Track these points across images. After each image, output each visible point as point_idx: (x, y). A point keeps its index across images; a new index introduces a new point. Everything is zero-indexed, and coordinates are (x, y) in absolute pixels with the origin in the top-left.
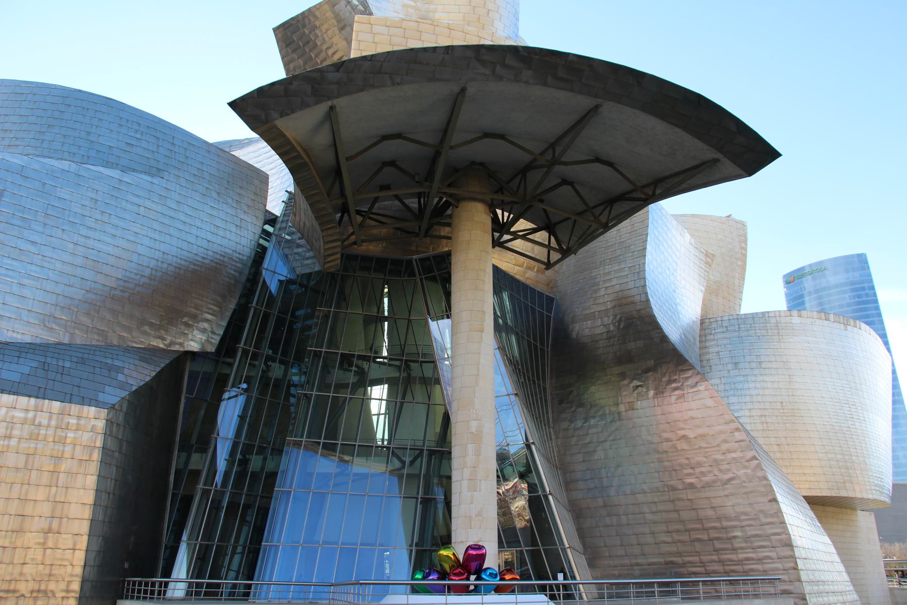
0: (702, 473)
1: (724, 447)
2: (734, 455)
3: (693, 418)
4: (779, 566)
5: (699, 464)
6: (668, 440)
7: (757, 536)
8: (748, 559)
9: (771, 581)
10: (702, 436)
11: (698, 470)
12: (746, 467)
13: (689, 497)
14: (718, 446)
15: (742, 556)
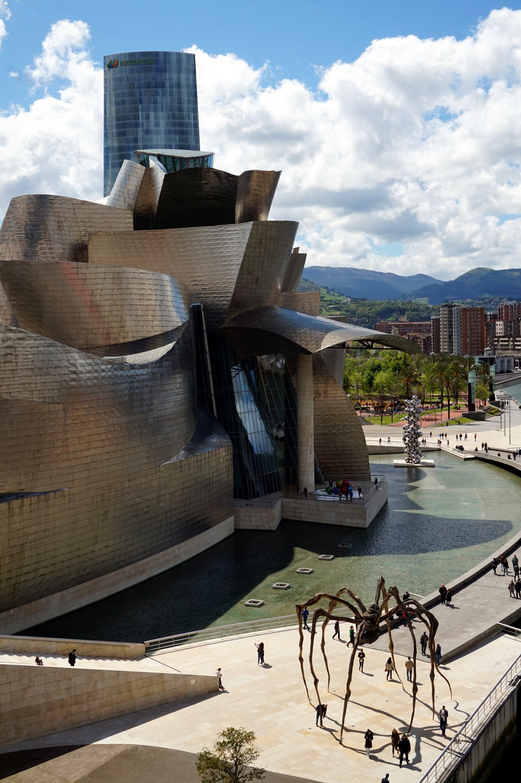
0: (339, 429)
1: (349, 420)
2: (352, 423)
3: (338, 407)
4: (363, 464)
5: (339, 426)
6: (327, 415)
7: (356, 453)
8: (352, 462)
9: (359, 470)
10: (341, 415)
11: (337, 428)
12: (356, 428)
13: (333, 438)
14: (347, 419)
15: (349, 461)
